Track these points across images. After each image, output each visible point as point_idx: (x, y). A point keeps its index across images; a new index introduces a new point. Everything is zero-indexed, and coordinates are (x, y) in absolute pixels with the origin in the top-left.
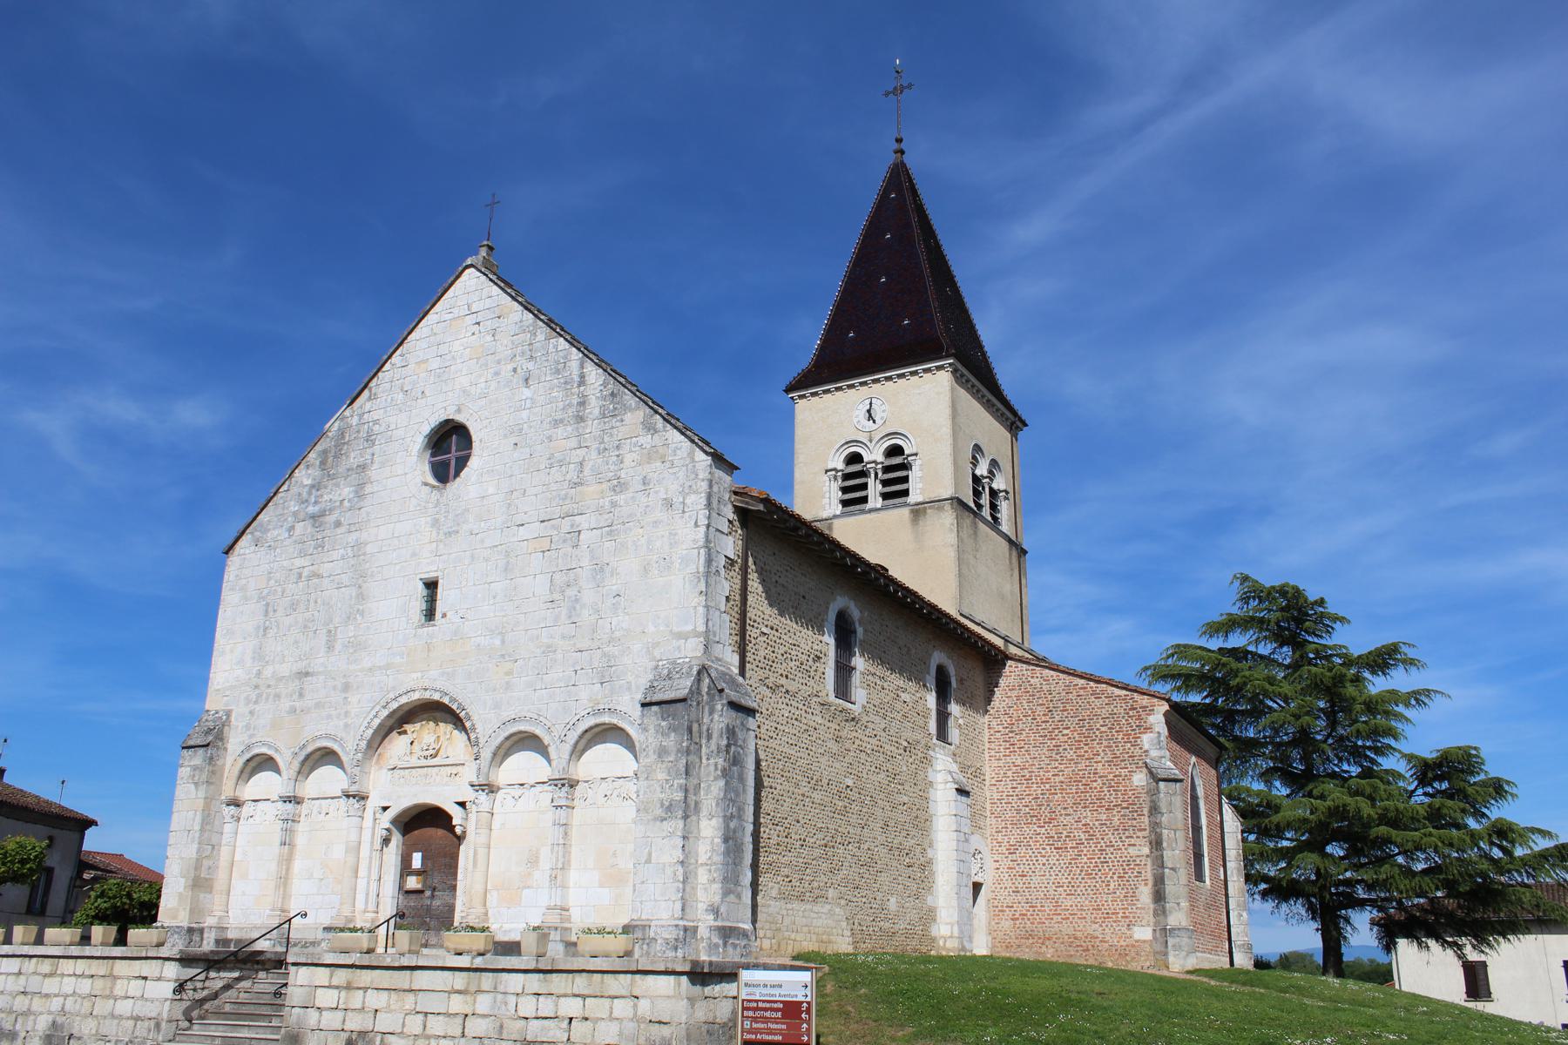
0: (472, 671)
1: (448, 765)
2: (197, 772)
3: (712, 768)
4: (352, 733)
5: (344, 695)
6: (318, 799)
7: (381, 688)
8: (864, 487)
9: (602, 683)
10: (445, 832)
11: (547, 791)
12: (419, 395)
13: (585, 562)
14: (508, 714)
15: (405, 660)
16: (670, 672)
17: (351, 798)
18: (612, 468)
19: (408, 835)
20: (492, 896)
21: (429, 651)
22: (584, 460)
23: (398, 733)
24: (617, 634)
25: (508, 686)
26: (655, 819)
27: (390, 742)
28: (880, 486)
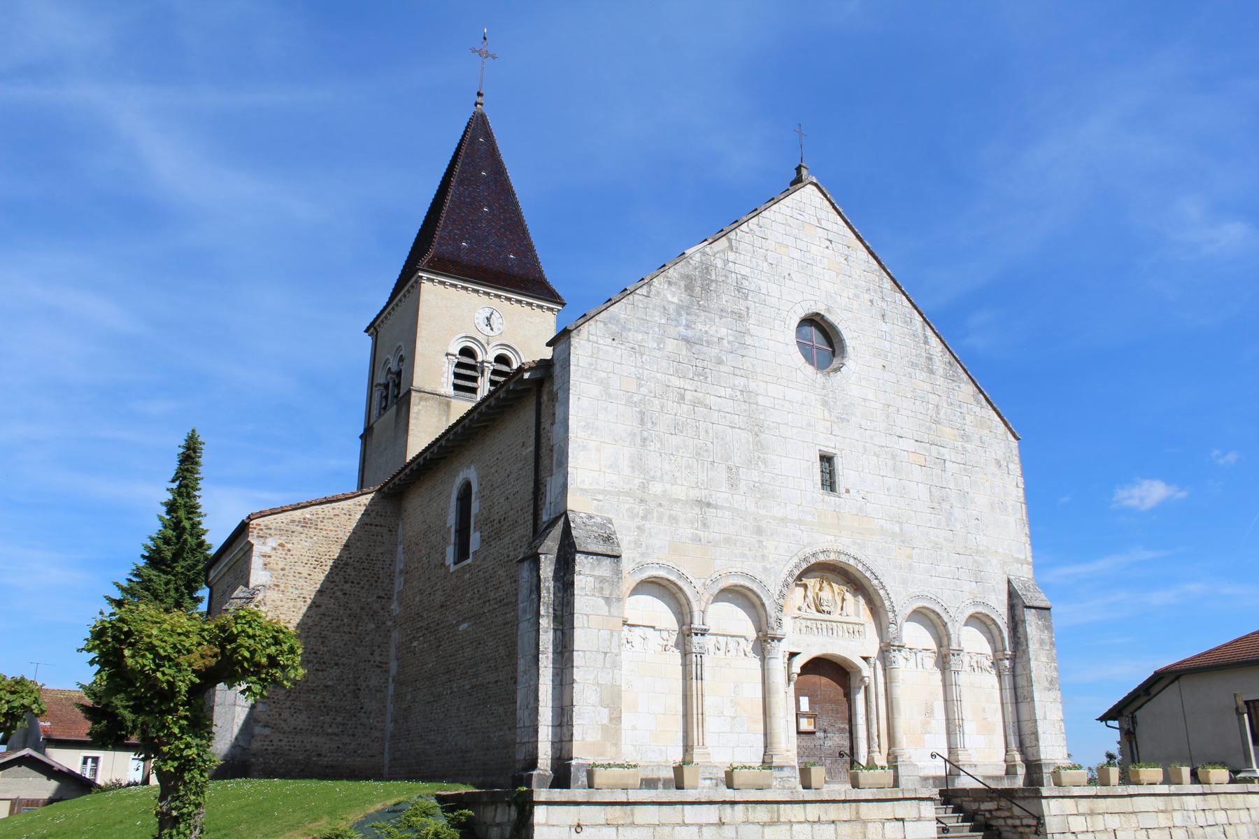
2: (606, 586)
4: (773, 577)
7: (798, 541)
10: (828, 679)
17: (776, 641)
21: (838, 520)
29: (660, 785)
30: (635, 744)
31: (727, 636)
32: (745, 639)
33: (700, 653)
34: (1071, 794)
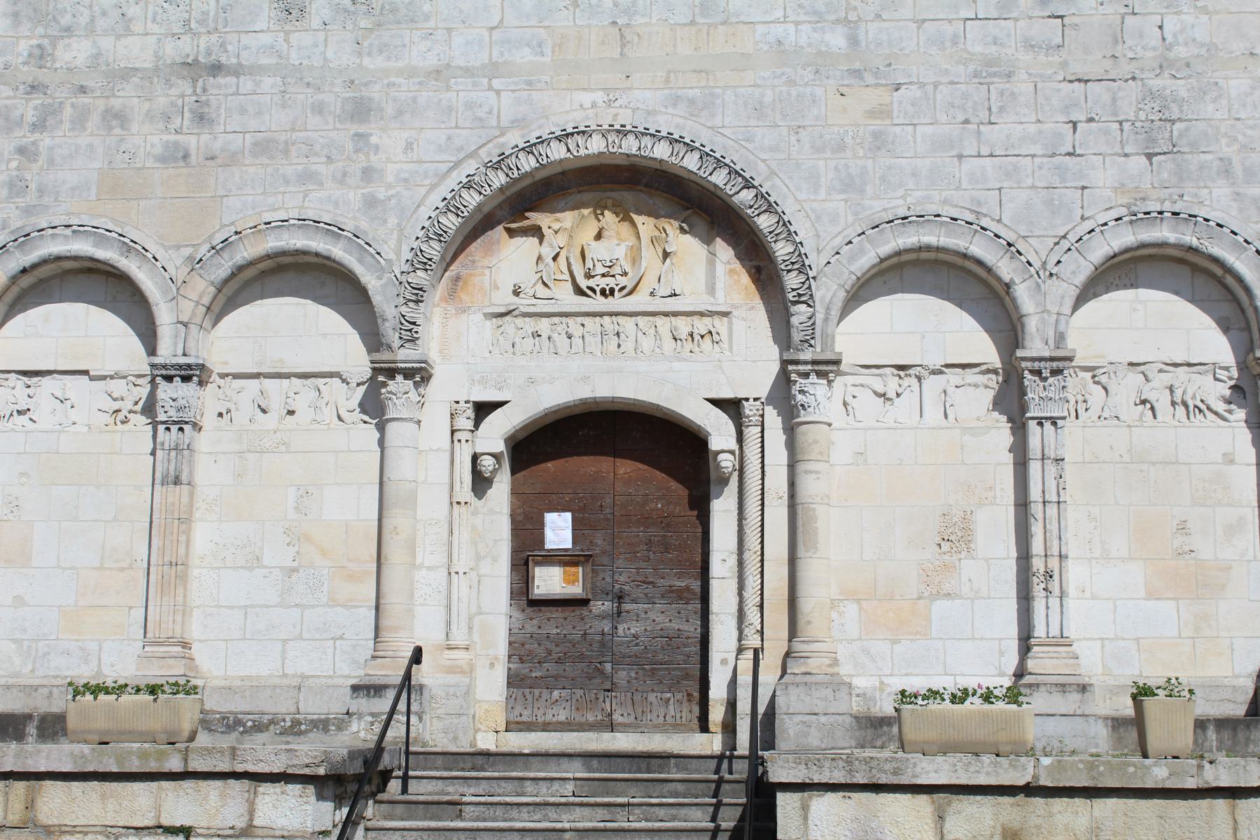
0: (768, 99)
1: (676, 314)
4: (393, 221)
5: (355, 128)
6: (256, 376)
7: (481, 119)
9: (1149, 156)
10: (640, 465)
11: (976, 386)
15: (547, 59)
17: (399, 378)
19: (524, 473)
20: (841, 614)
21: (623, 46)
23: (509, 231)
24: (1181, 52)
25: (879, 142)
27: (489, 250)
29: (32, 730)
30: (18, 636)
31: (288, 376)
32: (344, 381)
33: (175, 423)
34: (905, 780)
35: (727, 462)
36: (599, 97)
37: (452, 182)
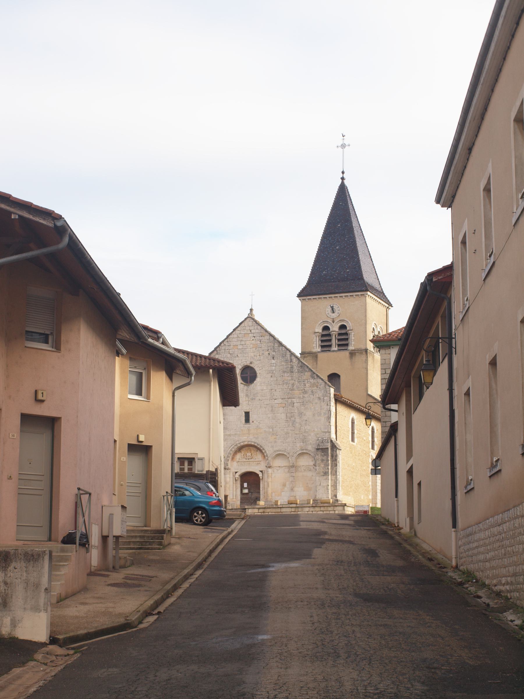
3: (334, 464)
8: (330, 340)
12: (236, 356)
13: (296, 411)
14: (275, 449)
16: (322, 441)
18: (302, 387)
22: (293, 384)
24: (307, 430)
25: (275, 442)
26: (322, 476)
28: (337, 341)
35: (261, 478)
36: (246, 437)
37: (231, 448)
